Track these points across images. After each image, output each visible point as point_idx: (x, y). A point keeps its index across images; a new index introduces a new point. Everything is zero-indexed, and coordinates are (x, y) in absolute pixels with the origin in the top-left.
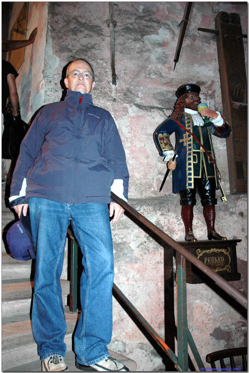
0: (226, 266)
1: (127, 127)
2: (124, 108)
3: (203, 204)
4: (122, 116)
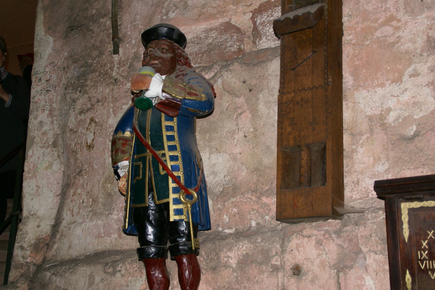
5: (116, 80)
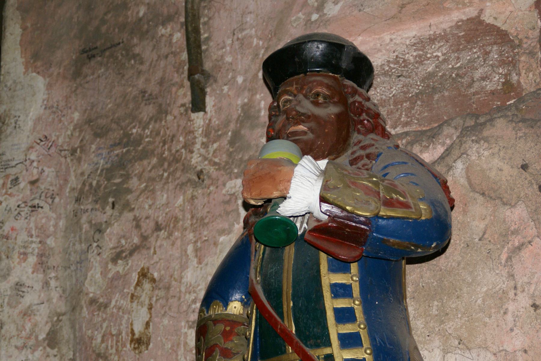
5: (199, 174)
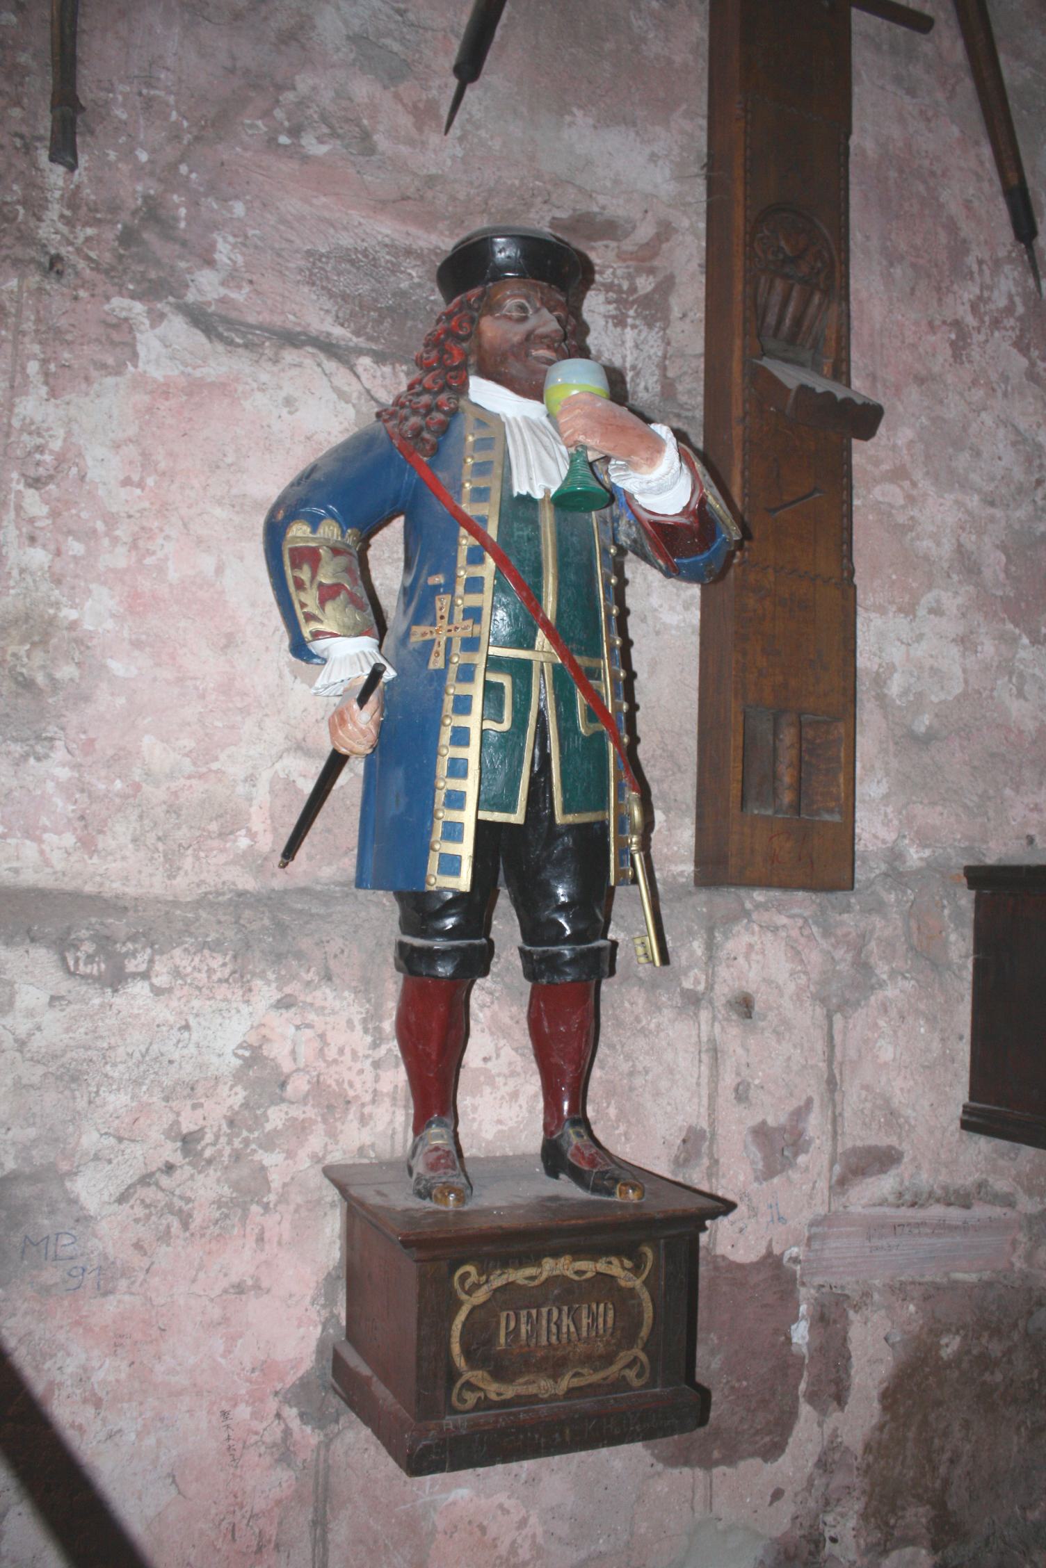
0: (624, 1357)
1: (117, 446)
2: (116, 327)
3: (534, 968)
4: (94, 374)
5: (55, 260)
